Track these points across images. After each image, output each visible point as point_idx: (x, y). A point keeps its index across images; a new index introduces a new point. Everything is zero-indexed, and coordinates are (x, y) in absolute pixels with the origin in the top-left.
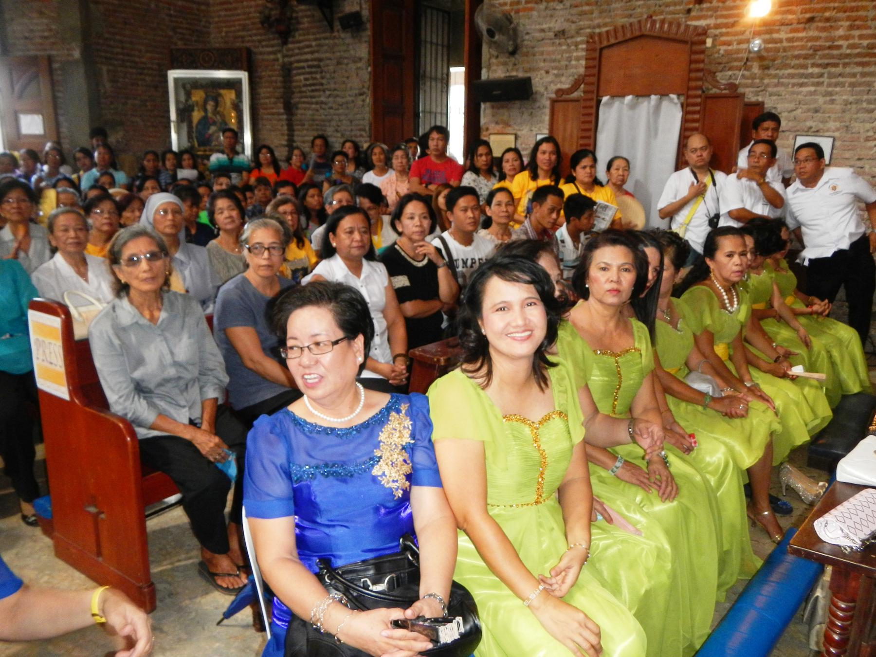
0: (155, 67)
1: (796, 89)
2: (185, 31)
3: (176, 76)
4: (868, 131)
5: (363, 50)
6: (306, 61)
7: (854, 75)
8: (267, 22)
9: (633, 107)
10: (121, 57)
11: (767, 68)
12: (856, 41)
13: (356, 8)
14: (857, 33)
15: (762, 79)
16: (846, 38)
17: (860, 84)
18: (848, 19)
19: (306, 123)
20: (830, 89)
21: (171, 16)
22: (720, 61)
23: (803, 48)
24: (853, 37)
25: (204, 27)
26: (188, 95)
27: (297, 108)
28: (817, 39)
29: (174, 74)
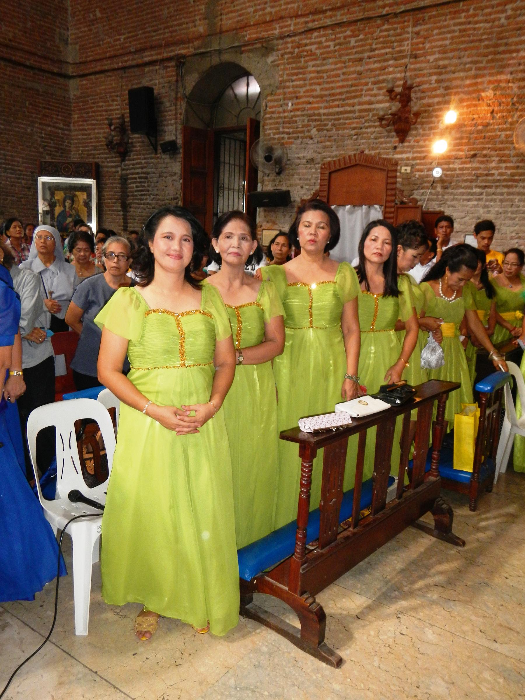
0: (29, 173)
1: (465, 203)
2: (52, 149)
3: (43, 181)
4: (512, 232)
5: (177, 167)
6: (138, 173)
7: (502, 194)
8: (110, 145)
9: (351, 213)
10: (4, 166)
11: (447, 188)
12: (504, 171)
13: (173, 138)
14: (504, 165)
15: (443, 195)
16: (497, 168)
17: (507, 200)
18: (498, 156)
19: (137, 218)
20: (487, 203)
21: (42, 137)
22: (416, 182)
23: (469, 174)
24: (501, 168)
25: (67, 146)
26: (52, 195)
27: (130, 207)
28: (478, 169)
29: (42, 179)
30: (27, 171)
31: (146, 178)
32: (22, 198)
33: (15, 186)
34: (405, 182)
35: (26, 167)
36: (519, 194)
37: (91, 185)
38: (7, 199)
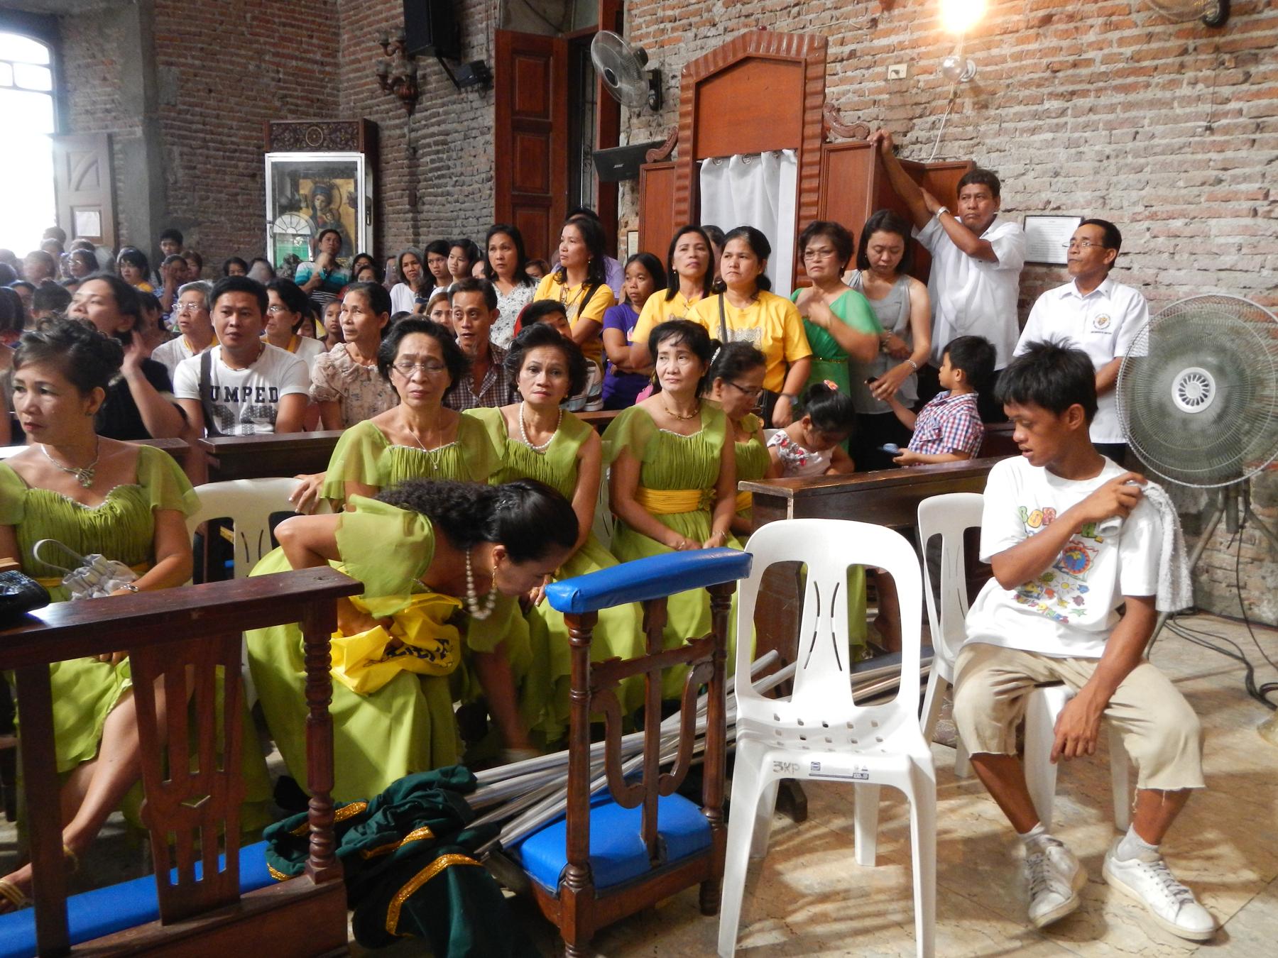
1: (1026, 138)
2: (299, 102)
3: (274, 160)
4: (1134, 204)
5: (488, 117)
6: (433, 135)
7: (1112, 109)
9: (743, 173)
10: (202, 135)
11: (986, 107)
12: (1115, 50)
13: (484, 57)
14: (1114, 35)
15: (976, 125)
17: (1122, 124)
19: (433, 224)
20: (1076, 135)
21: (279, 80)
22: (918, 99)
24: (1110, 44)
25: (329, 95)
26: (295, 187)
27: (424, 204)
29: (272, 158)
30: (248, 145)
31: (444, 143)
32: (237, 194)
33: (225, 173)
34: (897, 100)
35: (246, 138)
36: (1152, 104)
37: (355, 163)
38: (208, 198)
